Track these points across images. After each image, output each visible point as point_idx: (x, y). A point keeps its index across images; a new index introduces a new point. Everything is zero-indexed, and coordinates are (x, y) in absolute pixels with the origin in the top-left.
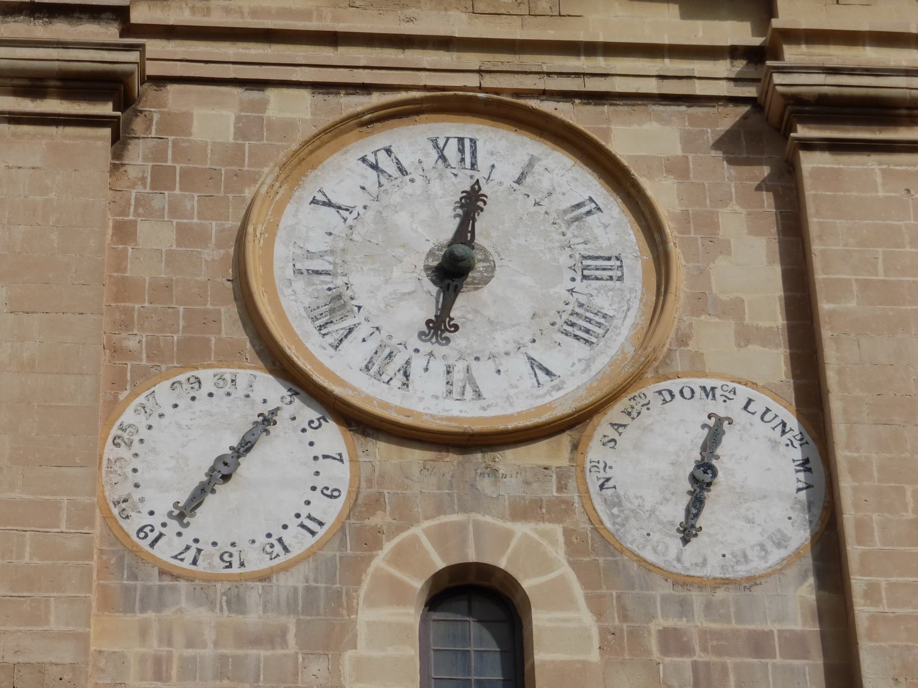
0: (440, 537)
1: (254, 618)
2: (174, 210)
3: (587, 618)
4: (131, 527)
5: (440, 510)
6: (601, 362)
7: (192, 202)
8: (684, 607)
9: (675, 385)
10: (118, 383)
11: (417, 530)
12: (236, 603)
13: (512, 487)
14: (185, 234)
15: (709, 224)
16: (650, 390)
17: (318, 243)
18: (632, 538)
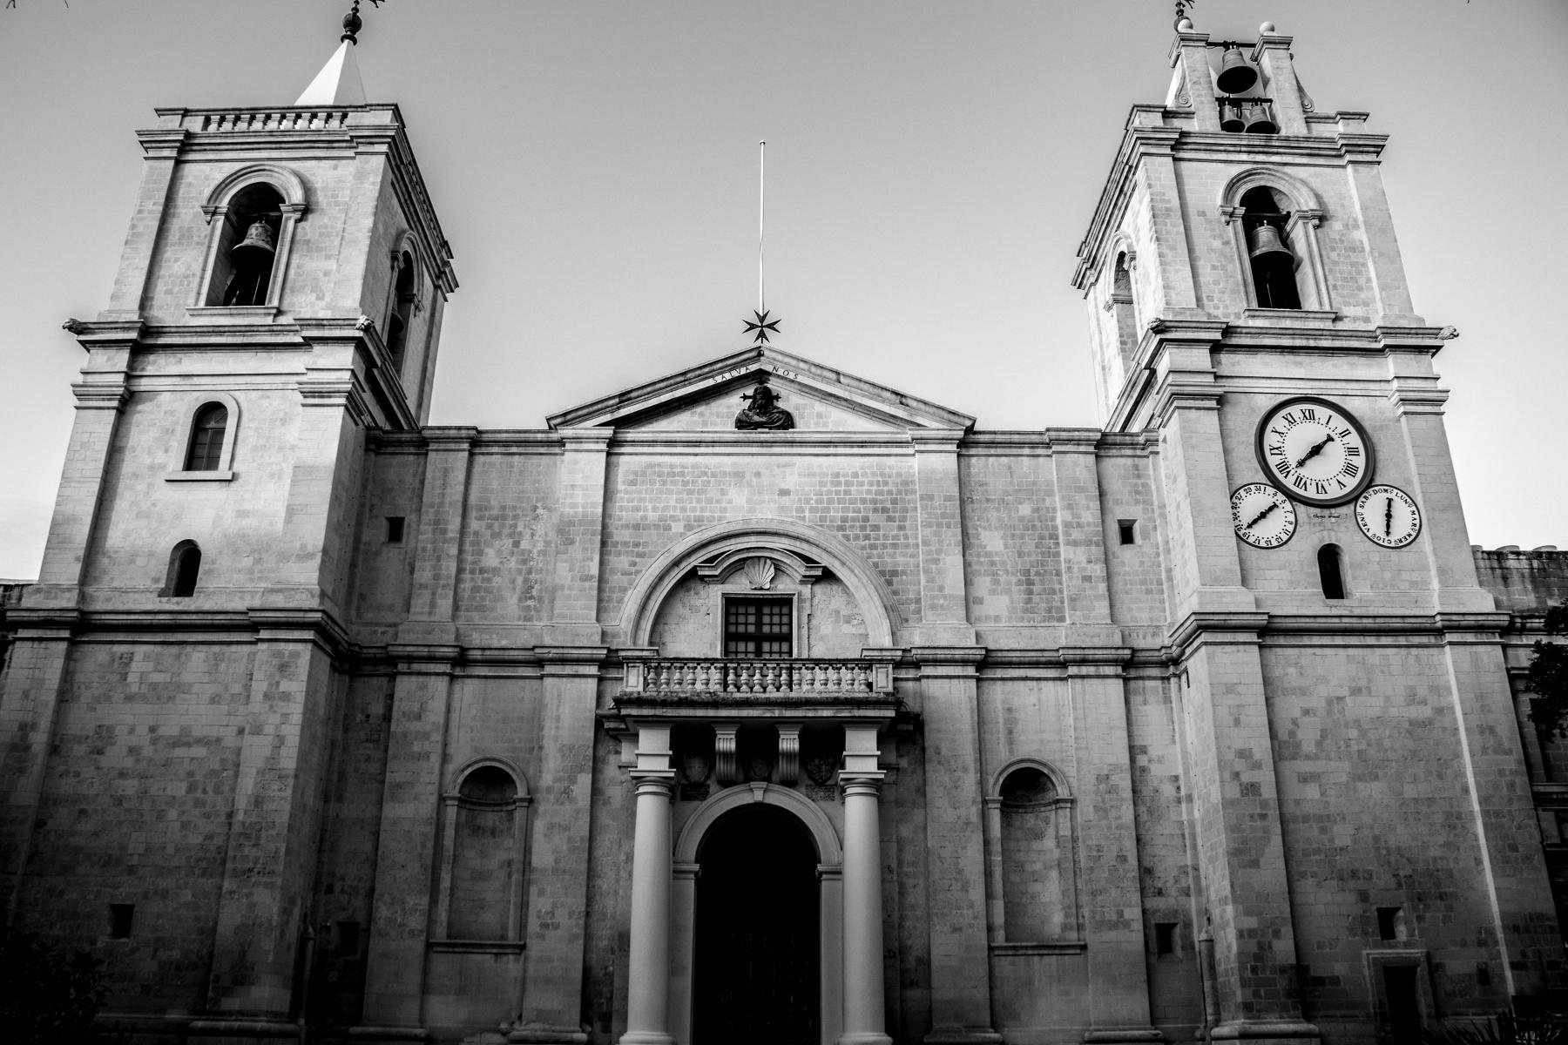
9: (1377, 488)
16: (1371, 490)
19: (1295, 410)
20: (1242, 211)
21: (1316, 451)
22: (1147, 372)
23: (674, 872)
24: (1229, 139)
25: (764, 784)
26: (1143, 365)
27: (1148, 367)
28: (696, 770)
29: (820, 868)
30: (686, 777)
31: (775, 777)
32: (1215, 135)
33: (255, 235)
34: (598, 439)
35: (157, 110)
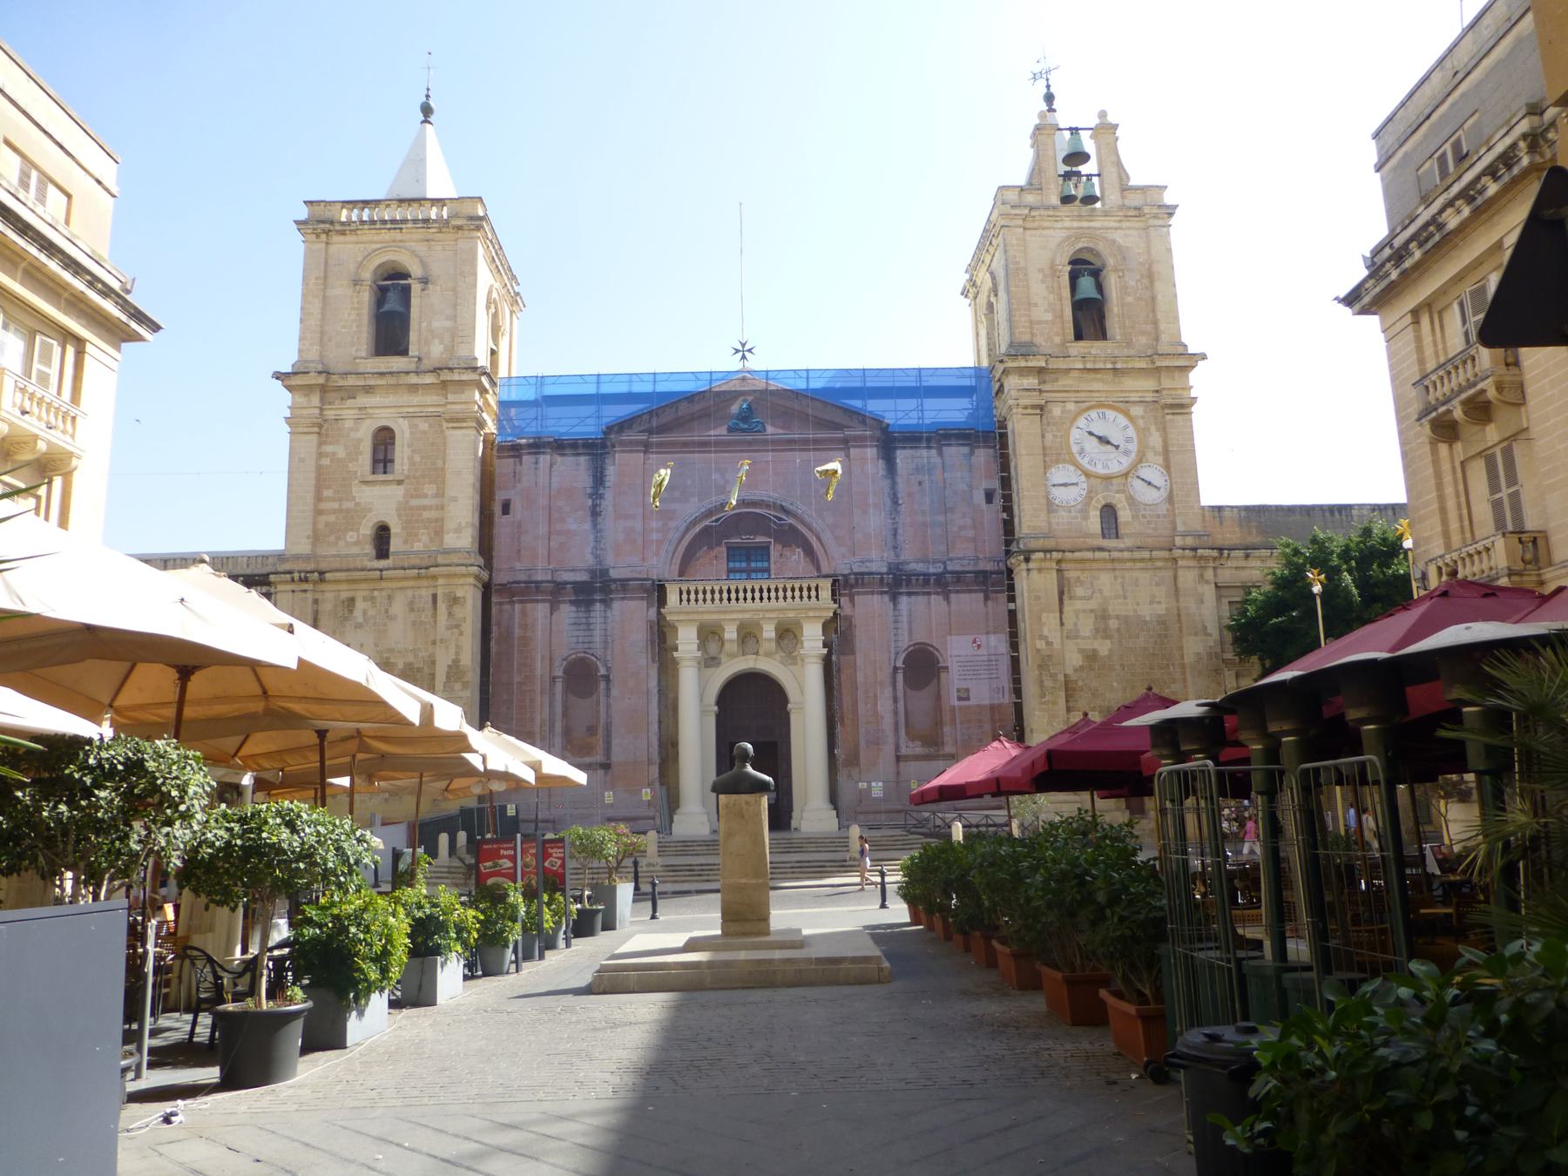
0: (1104, 498)
1: (1073, 514)
2: (1052, 431)
3: (1129, 512)
4: (1050, 497)
5: (1103, 492)
6: (1130, 460)
7: (1054, 428)
8: (1145, 509)
10: (1045, 468)
11: (1099, 496)
12: (1070, 512)
13: (1115, 488)
14: (1055, 436)
15: (1148, 429)
17: (1078, 437)
18: (1137, 497)
19: (1093, 414)
20: (1069, 268)
21: (1104, 440)
22: (998, 385)
23: (703, 713)
24: (1067, 209)
25: (754, 656)
26: (996, 379)
27: (999, 380)
28: (713, 648)
29: (790, 706)
30: (707, 653)
31: (760, 652)
32: (1054, 208)
33: (392, 304)
34: (638, 443)
35: (305, 202)
